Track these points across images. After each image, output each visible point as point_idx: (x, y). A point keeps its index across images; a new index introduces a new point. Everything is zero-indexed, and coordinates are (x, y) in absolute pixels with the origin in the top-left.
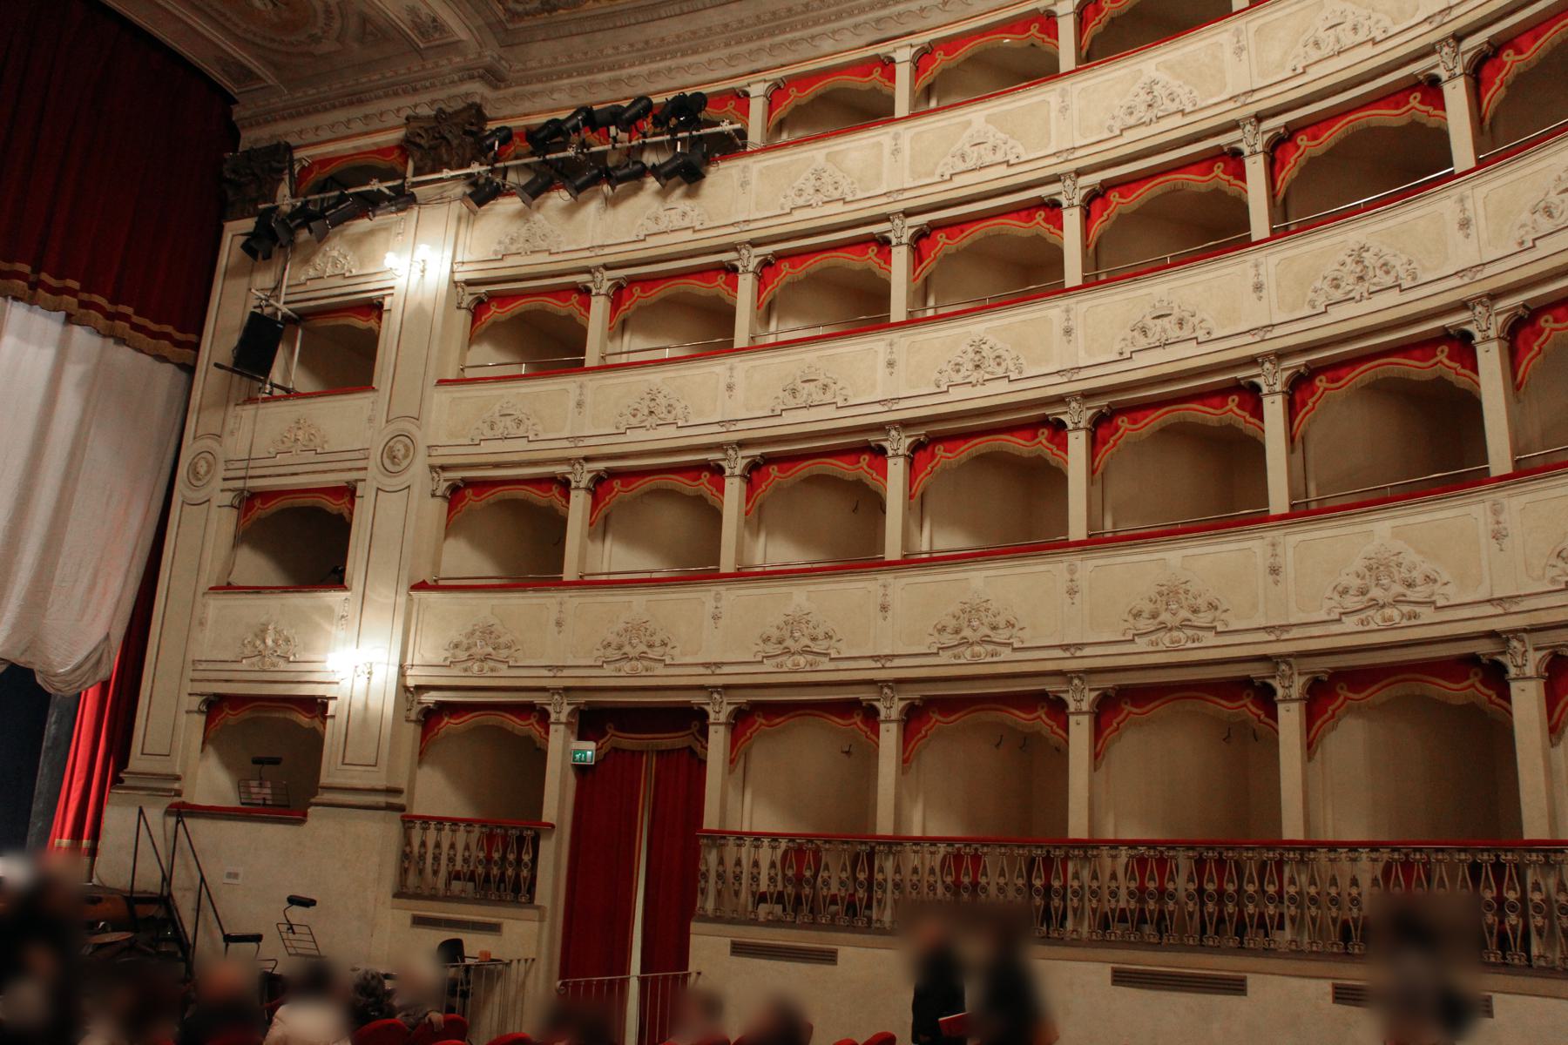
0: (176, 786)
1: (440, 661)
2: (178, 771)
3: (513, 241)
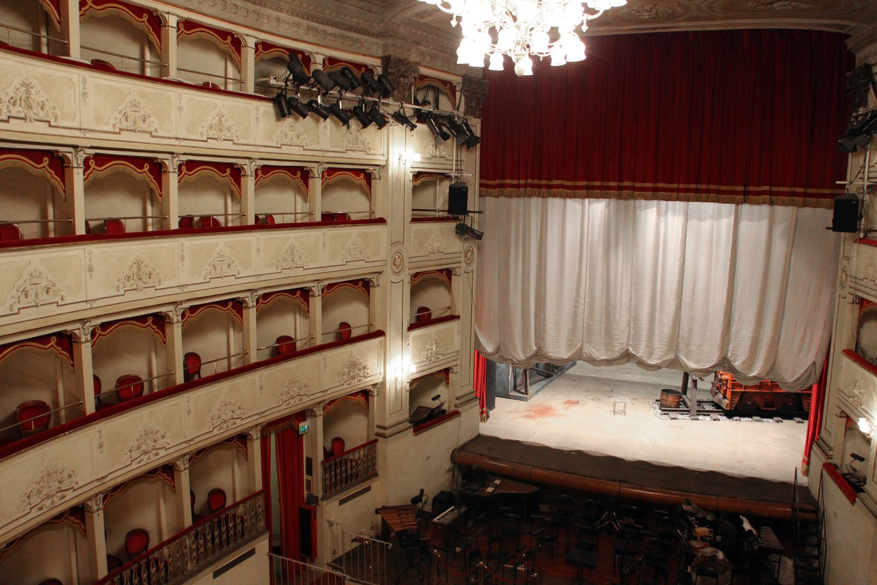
0: (831, 453)
2: (832, 445)
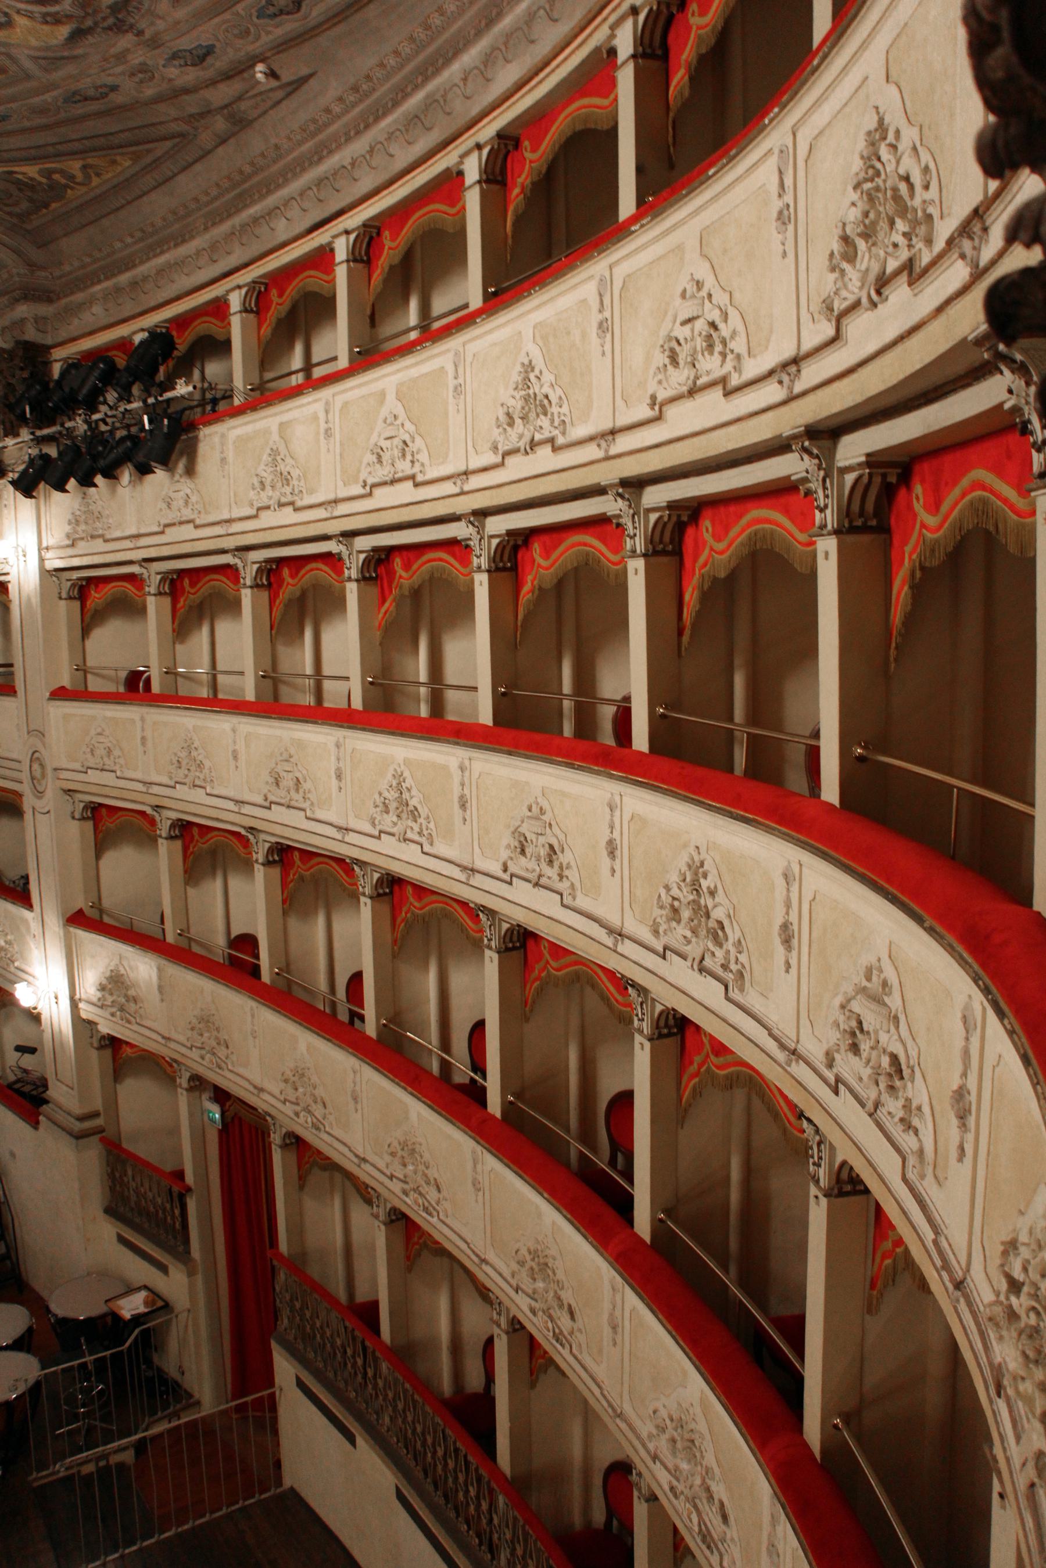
1: (95, 1000)
3: (77, 523)
